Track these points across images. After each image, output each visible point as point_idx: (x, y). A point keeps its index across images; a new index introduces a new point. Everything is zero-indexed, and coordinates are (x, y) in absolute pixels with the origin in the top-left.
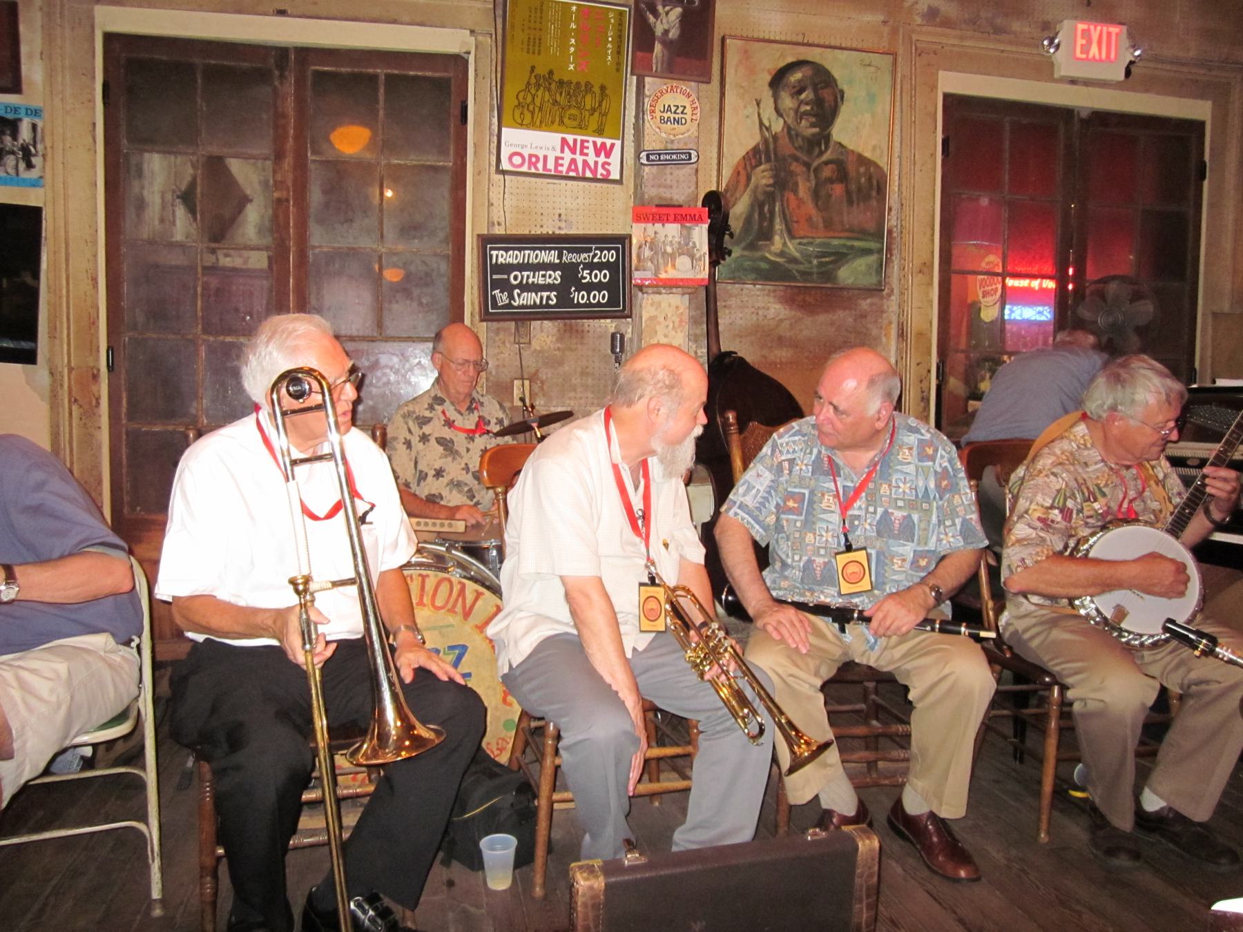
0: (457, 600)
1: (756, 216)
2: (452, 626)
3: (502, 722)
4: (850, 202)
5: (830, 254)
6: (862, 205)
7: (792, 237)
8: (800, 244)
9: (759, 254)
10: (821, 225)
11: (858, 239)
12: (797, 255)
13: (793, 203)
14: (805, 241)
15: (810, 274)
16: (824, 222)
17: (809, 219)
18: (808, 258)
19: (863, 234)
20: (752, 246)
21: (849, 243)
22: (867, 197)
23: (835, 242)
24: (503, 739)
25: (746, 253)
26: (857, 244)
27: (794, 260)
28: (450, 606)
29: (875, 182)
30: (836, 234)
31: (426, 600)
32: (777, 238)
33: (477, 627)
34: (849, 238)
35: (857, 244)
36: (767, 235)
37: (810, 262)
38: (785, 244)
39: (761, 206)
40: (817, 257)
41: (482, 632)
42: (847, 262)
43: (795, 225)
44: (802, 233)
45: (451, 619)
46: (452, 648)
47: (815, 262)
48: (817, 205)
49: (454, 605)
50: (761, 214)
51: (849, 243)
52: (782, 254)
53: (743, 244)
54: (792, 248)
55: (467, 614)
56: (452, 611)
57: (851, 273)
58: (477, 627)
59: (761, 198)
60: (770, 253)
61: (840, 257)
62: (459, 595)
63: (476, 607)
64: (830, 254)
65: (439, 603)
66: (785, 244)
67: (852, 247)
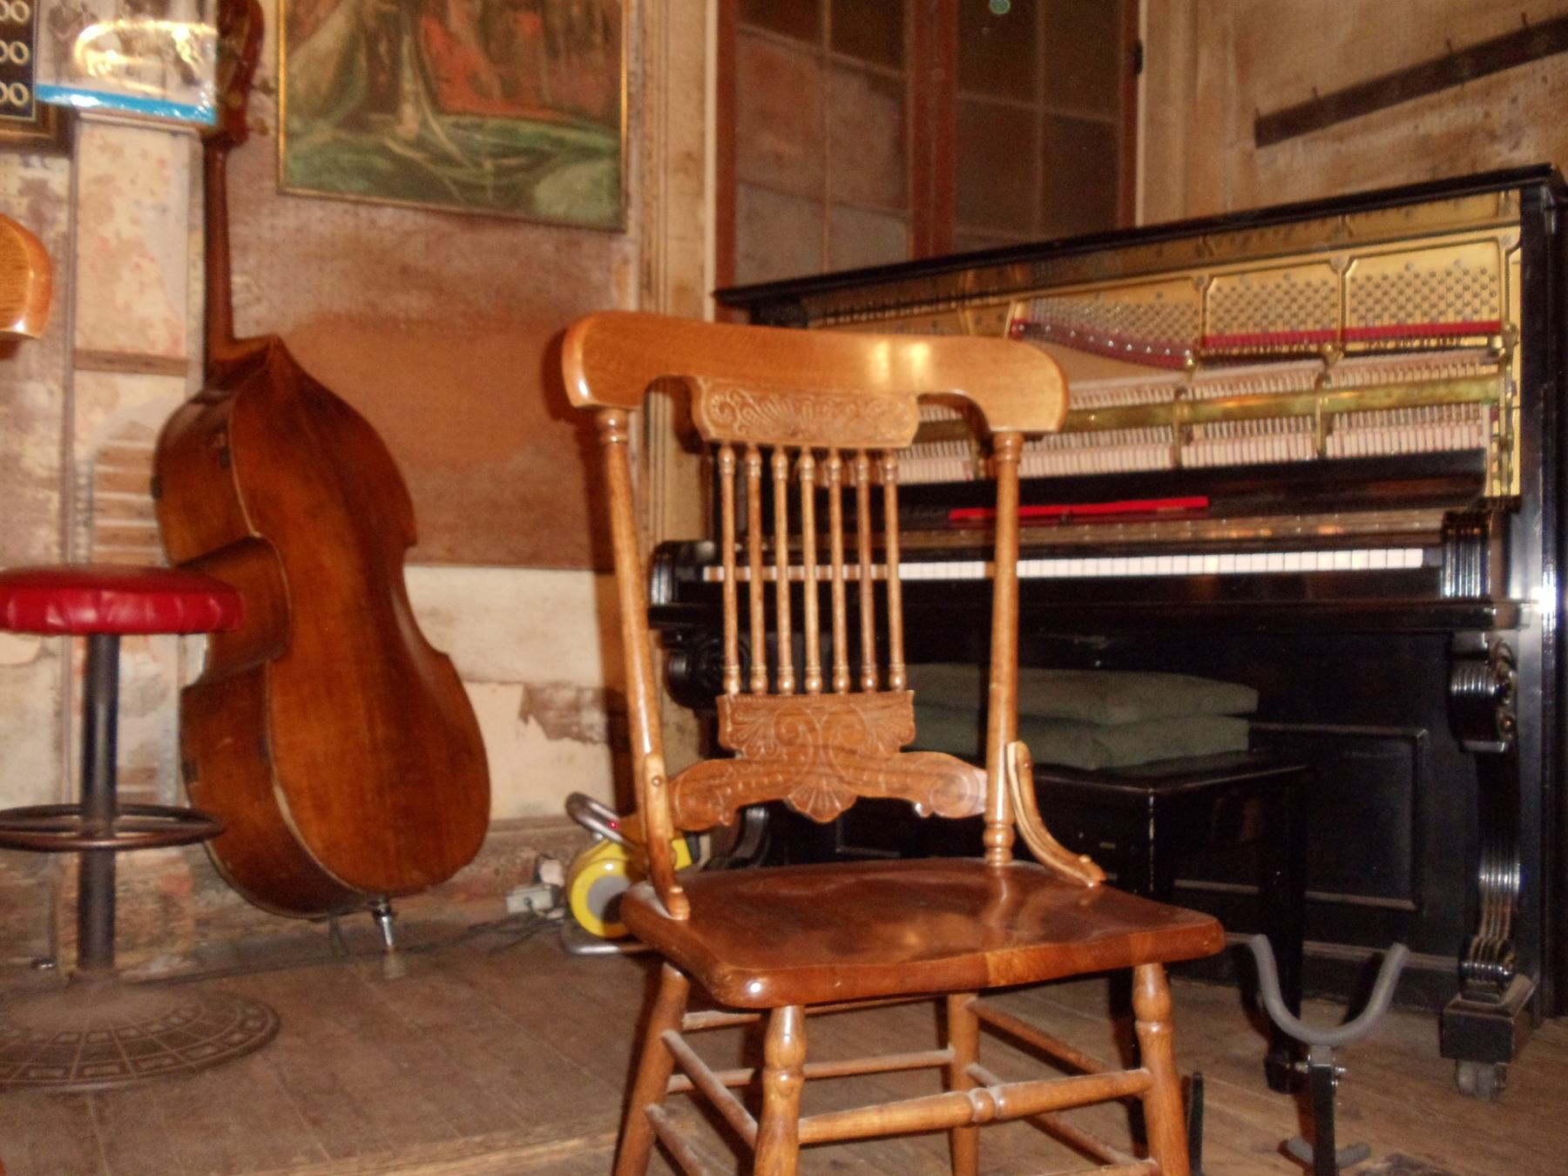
1: (362, 60)
4: (553, 53)
5: (517, 152)
6: (575, 60)
7: (439, 107)
8: (457, 126)
9: (368, 140)
10: (497, 91)
11: (570, 126)
12: (452, 148)
13: (438, 43)
14: (466, 120)
15: (482, 188)
16: (503, 83)
17: (473, 79)
18: (474, 156)
19: (578, 116)
20: (356, 123)
21: (556, 133)
22: (584, 45)
23: (527, 129)
25: (344, 135)
26: (572, 136)
27: (446, 159)
29: (598, 18)
30: (527, 113)
32: (408, 110)
34: (555, 123)
35: (572, 136)
36: (385, 100)
37: (479, 165)
38: (424, 124)
39: (372, 40)
40: (493, 156)
42: (553, 170)
43: (444, 86)
44: (458, 105)
47: (489, 165)
48: (487, 50)
50: (373, 56)
51: (556, 133)
52: (420, 143)
53: (339, 114)
54: (440, 131)
57: (563, 191)
59: (371, 23)
60: (395, 138)
61: (539, 160)
64: (517, 152)
66: (424, 124)
67: (560, 143)
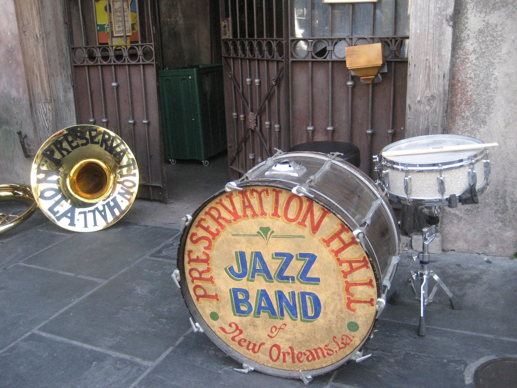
0: (306, 215)
2: (303, 237)
3: (347, 322)
24: (347, 337)
28: (300, 220)
31: (280, 212)
33: (324, 240)
41: (328, 246)
45: (300, 231)
46: (303, 255)
49: (304, 220)
55: (315, 228)
56: (302, 224)
58: (324, 240)
62: (307, 212)
63: (323, 223)
65: (291, 215)
